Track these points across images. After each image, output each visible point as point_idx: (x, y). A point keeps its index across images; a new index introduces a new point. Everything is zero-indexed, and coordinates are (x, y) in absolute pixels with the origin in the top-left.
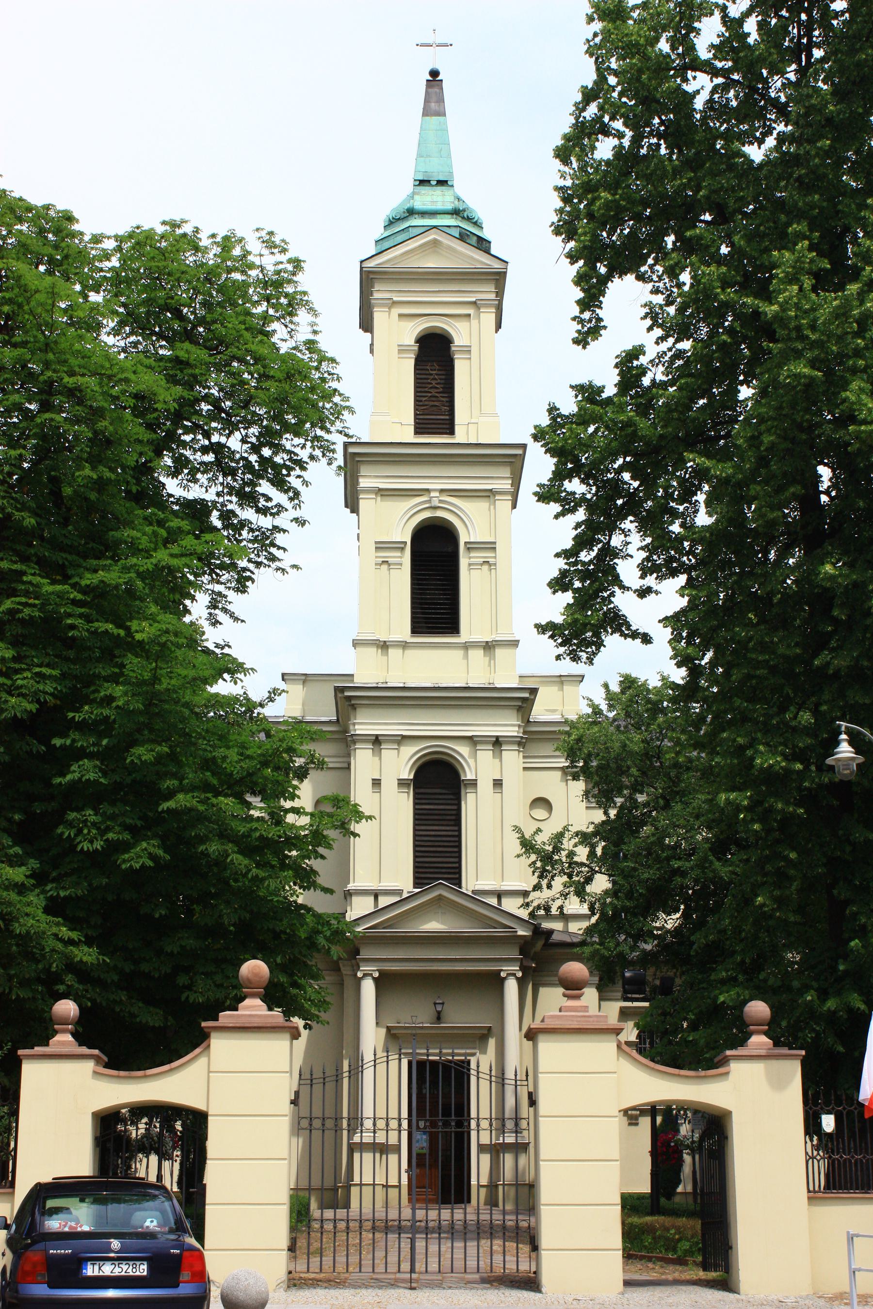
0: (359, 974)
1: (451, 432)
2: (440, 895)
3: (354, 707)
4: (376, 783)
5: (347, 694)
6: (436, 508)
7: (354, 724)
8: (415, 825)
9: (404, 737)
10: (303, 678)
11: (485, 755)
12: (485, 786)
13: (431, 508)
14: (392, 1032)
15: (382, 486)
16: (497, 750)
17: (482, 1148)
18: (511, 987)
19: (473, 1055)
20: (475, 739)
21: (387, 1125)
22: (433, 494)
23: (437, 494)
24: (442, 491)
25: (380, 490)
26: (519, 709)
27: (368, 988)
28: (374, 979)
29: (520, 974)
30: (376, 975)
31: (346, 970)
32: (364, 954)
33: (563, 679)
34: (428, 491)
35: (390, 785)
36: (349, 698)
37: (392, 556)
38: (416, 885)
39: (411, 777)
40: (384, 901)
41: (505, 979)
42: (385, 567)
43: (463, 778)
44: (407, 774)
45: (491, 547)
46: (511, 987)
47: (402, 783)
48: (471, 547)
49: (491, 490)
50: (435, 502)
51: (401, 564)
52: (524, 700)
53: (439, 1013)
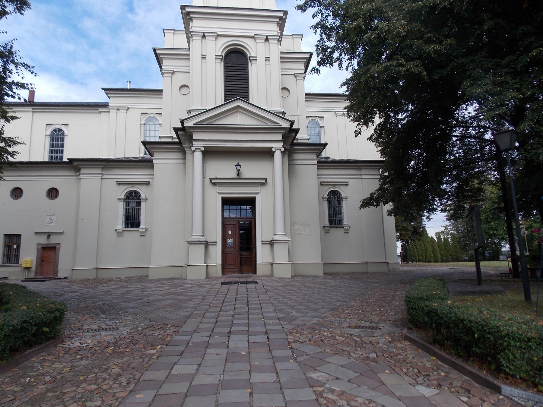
2: (238, 107)
3: (191, 19)
4: (204, 57)
5: (187, 9)
7: (192, 28)
8: (225, 81)
9: (219, 36)
10: (173, 31)
11: (261, 44)
12: (261, 59)
14: (213, 181)
16: (267, 43)
17: (263, 243)
18: (278, 156)
19: (257, 194)
20: (255, 36)
26: (278, 24)
27: (198, 156)
28: (202, 151)
29: (283, 149)
30: (203, 149)
31: (187, 150)
32: (196, 136)
33: (293, 36)
35: (211, 58)
36: (188, 13)
38: (225, 100)
39: (223, 54)
41: (275, 152)
43: (249, 56)
44: (220, 52)
46: (278, 156)
47: (217, 58)
52: (280, 18)
53: (238, 171)
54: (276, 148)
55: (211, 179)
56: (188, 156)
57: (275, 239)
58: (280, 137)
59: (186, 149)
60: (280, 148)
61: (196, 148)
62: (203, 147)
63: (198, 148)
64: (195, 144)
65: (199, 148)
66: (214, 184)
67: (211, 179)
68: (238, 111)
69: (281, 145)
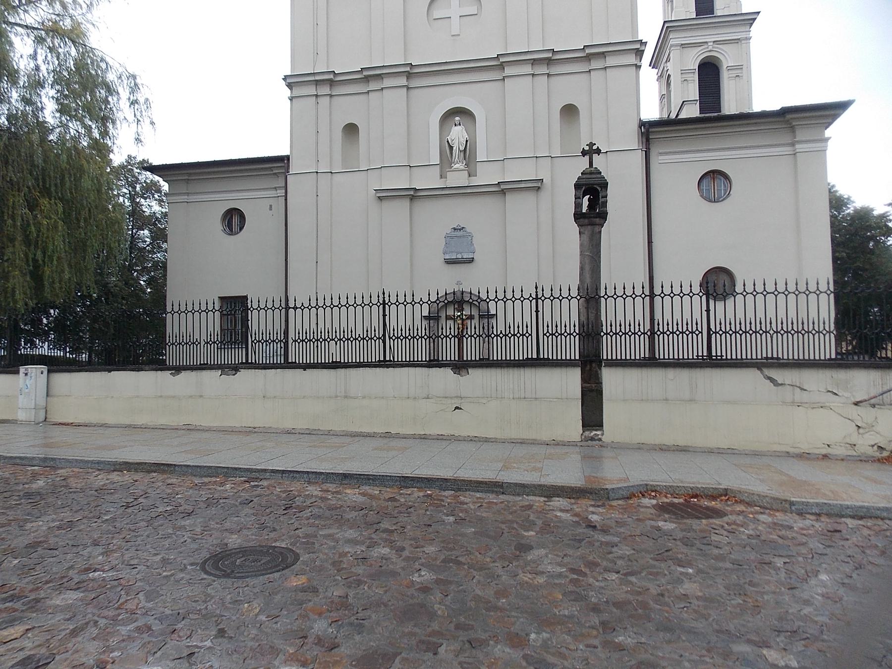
1: (713, 14)
6: (710, 51)
13: (710, 51)
15: (683, 42)
22: (709, 44)
23: (712, 44)
24: (714, 42)
25: (682, 44)
34: (706, 42)
37: (689, 77)
42: (685, 82)
45: (740, 67)
48: (729, 69)
49: (739, 39)
50: (710, 48)
51: (694, 80)
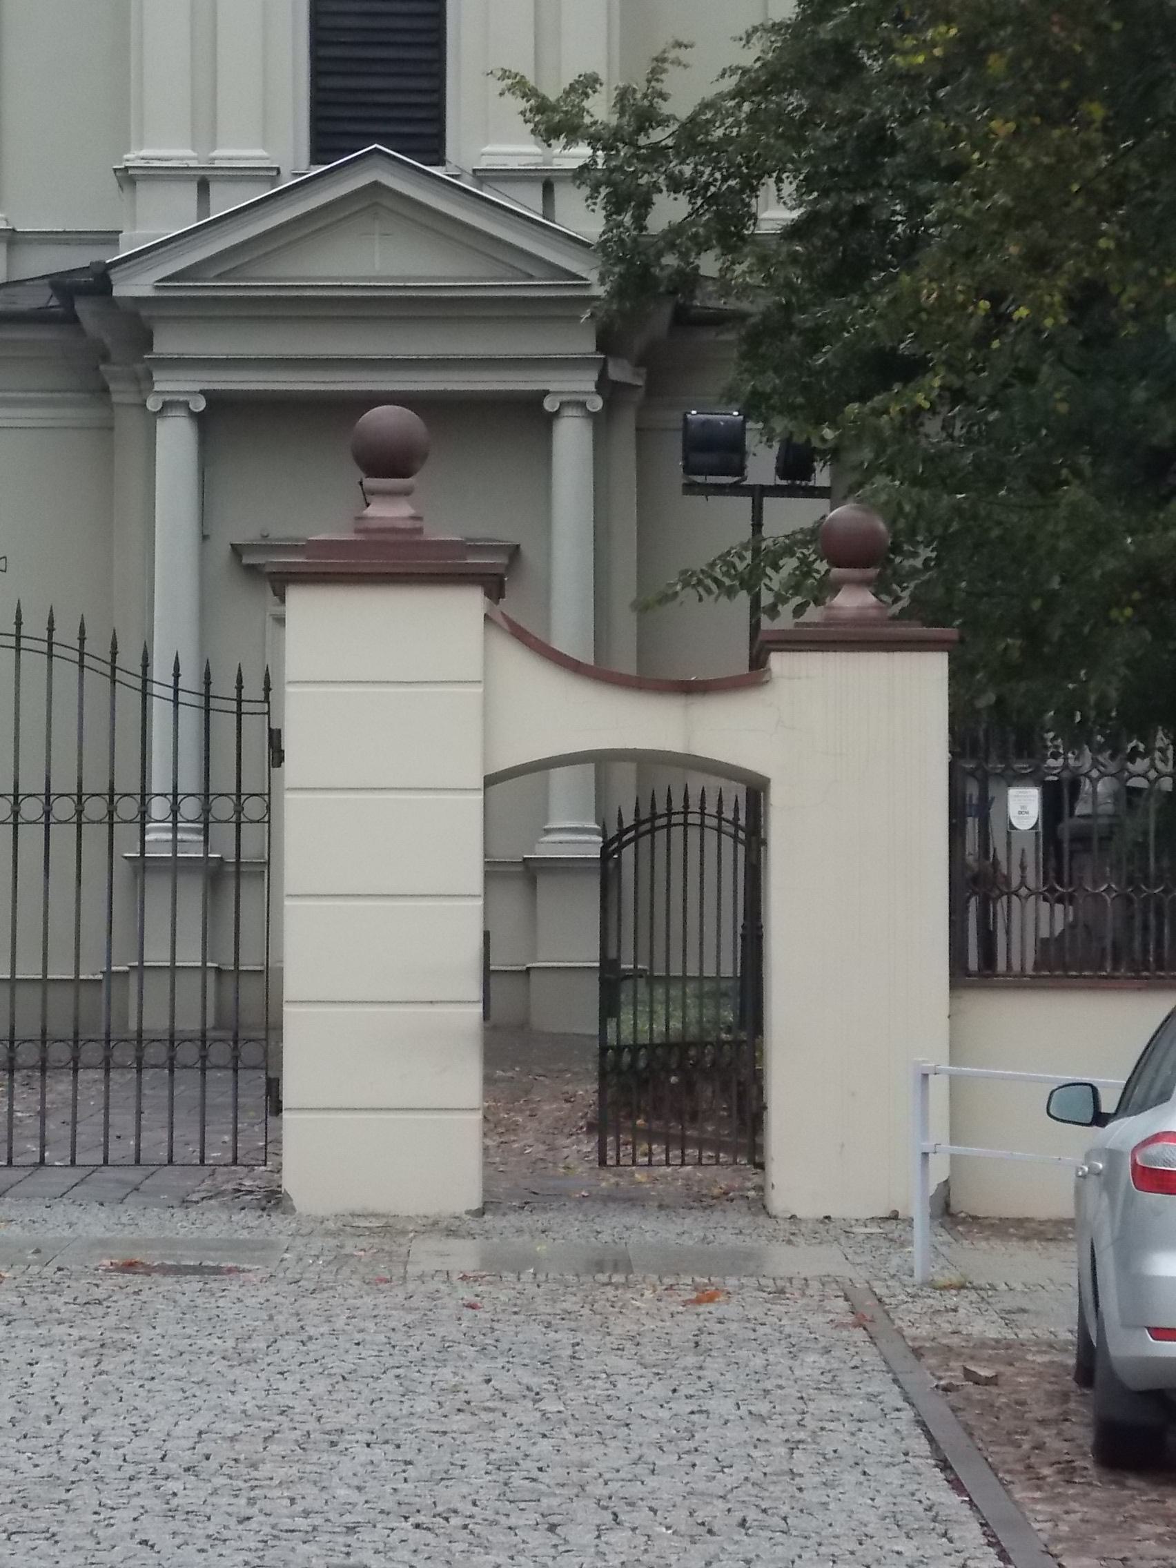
0: (153, 404)
2: (376, 184)
14: (247, 560)
21: (239, 809)
28: (195, 416)
29: (597, 404)
30: (200, 405)
31: (121, 393)
32: (167, 343)
40: (225, 201)
41: (556, 414)
54: (565, 398)
55: (237, 550)
56: (127, 422)
57: (542, 852)
58: (585, 345)
59: (112, 387)
60: (581, 398)
61: (168, 398)
62: (202, 392)
63: (175, 398)
64: (167, 383)
65: (182, 398)
66: (252, 570)
67: (237, 550)
68: (376, 204)
69: (585, 382)
